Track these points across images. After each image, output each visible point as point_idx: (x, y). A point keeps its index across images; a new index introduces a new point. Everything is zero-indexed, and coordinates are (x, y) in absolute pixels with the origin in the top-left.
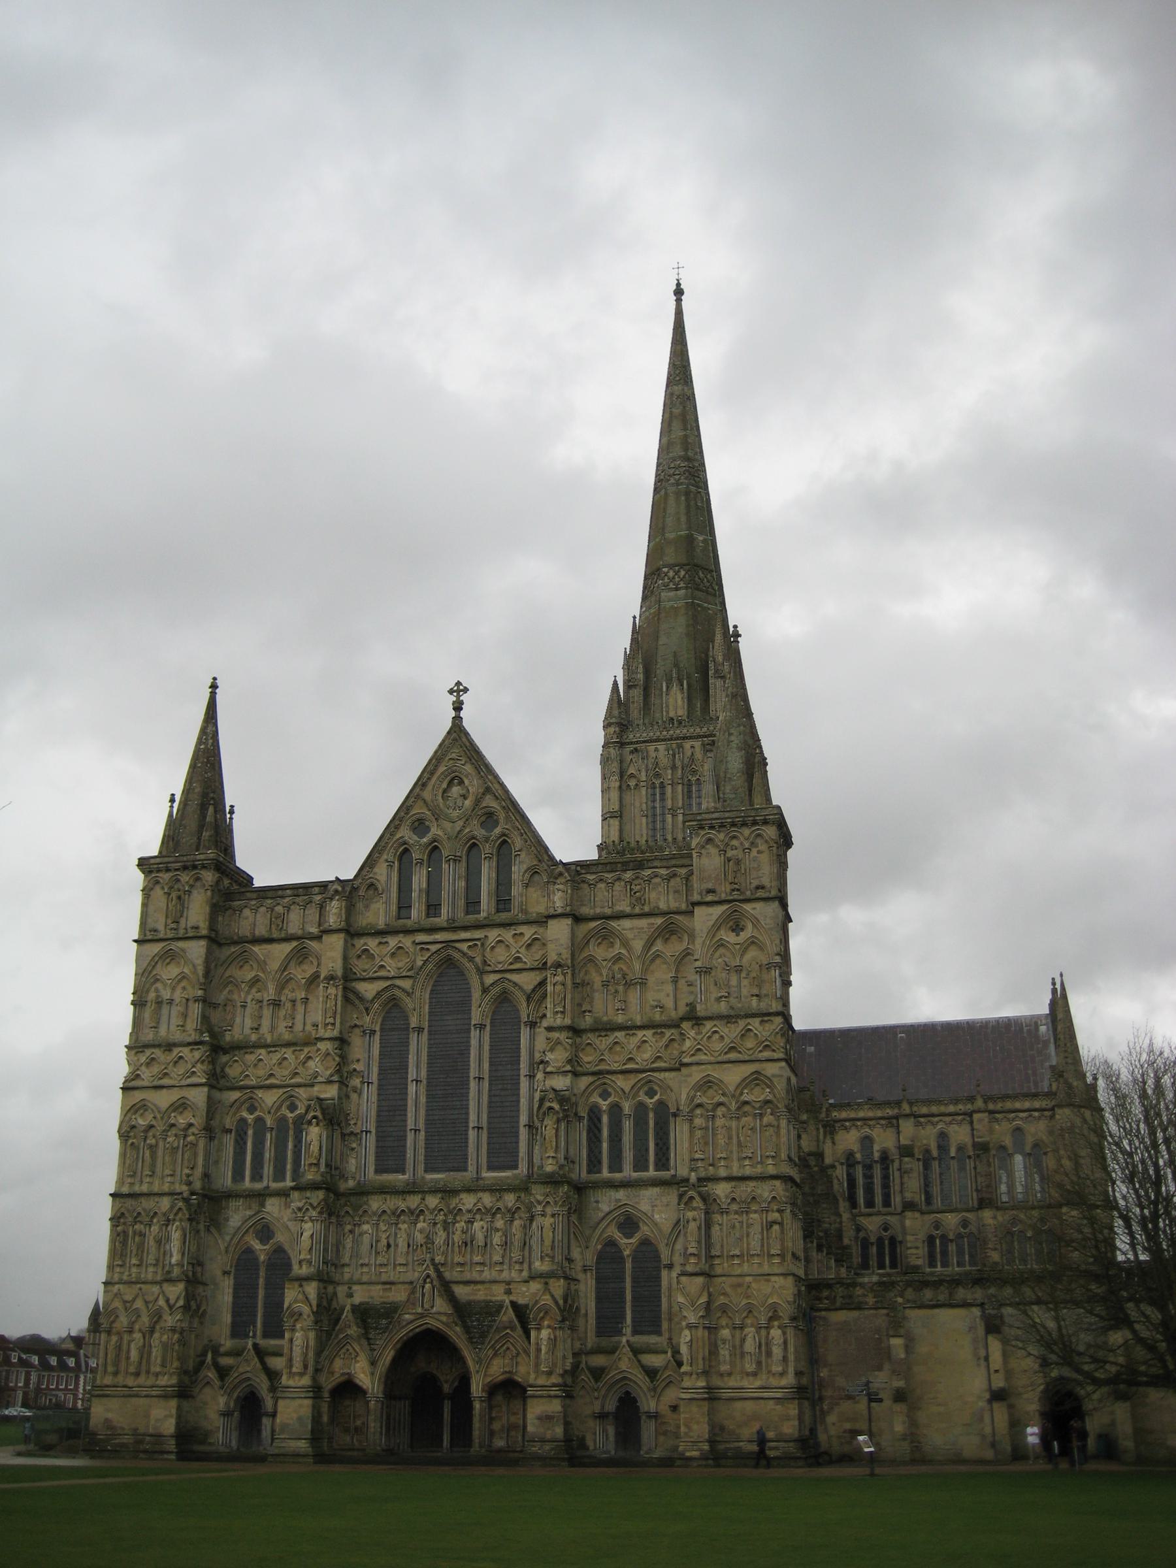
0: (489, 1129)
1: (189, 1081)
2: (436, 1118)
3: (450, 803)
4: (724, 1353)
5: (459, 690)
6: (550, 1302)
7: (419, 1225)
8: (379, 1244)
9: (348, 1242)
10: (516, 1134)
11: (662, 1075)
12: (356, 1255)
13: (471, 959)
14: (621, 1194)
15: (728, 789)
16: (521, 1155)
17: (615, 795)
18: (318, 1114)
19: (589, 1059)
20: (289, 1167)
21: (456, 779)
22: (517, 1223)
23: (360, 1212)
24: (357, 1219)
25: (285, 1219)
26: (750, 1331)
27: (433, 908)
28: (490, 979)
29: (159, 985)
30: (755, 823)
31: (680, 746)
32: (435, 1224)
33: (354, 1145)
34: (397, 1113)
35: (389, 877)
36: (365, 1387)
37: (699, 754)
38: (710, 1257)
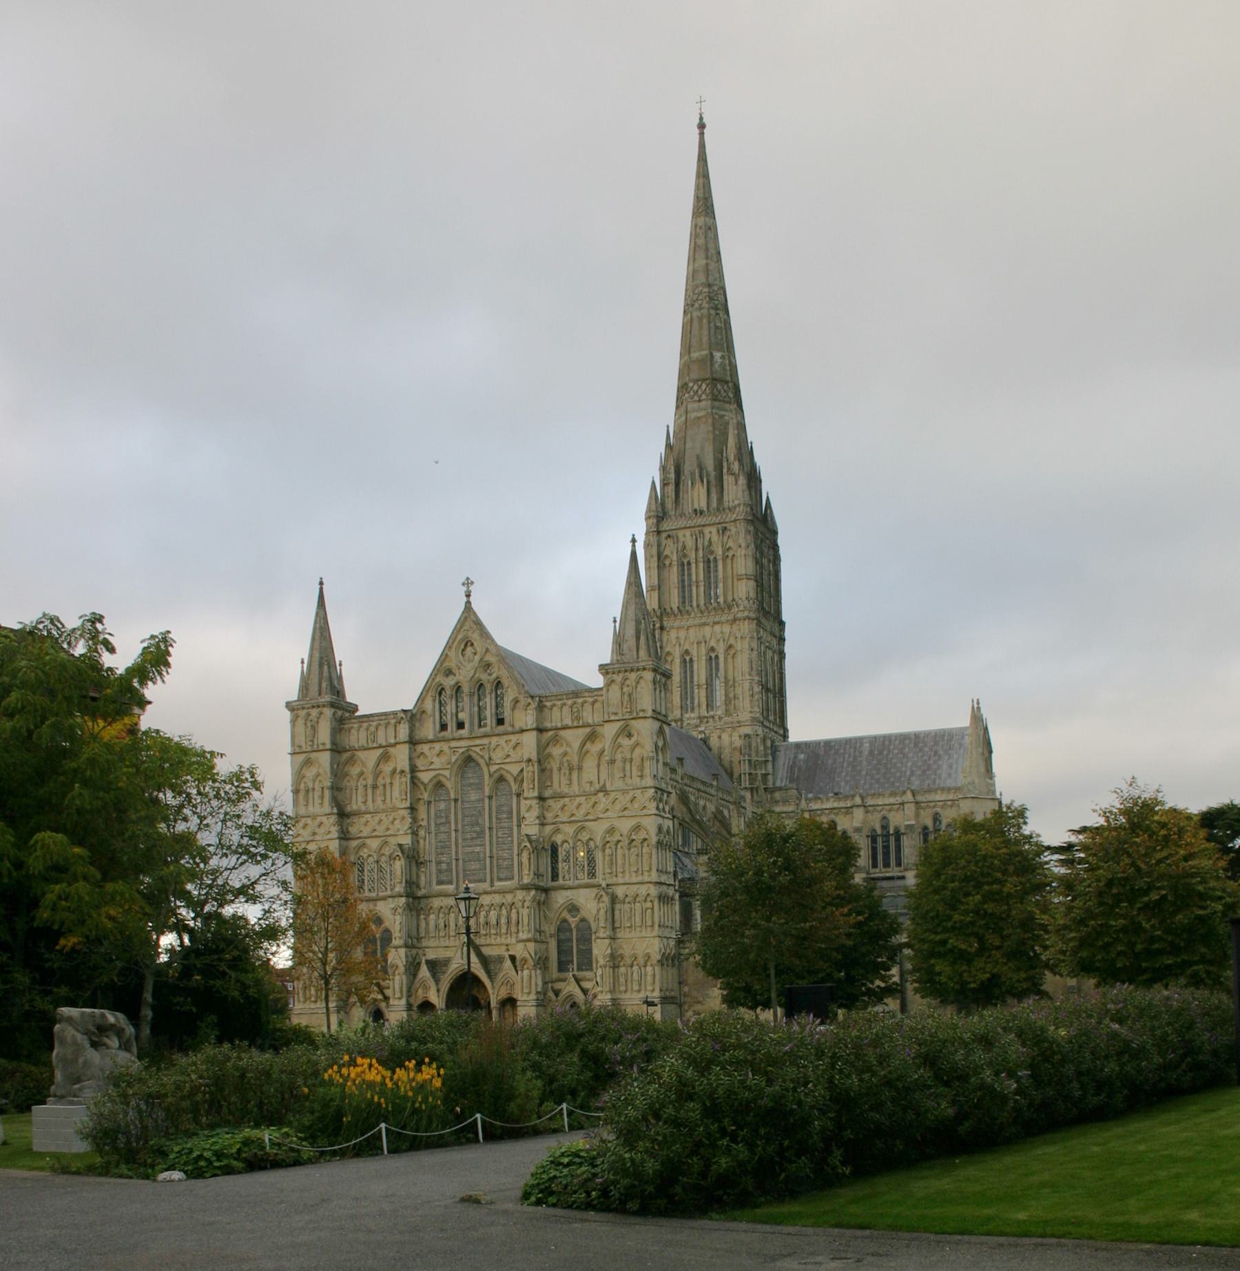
1: (329, 836)
3: (466, 657)
4: (622, 980)
5: (468, 583)
6: (528, 956)
12: (427, 932)
13: (482, 757)
14: (569, 893)
15: (625, 646)
17: (655, 572)
18: (400, 854)
21: (468, 643)
26: (635, 968)
27: (461, 725)
28: (493, 768)
29: (305, 780)
30: (638, 670)
31: (701, 532)
35: (434, 707)
37: (715, 538)
38: (614, 929)
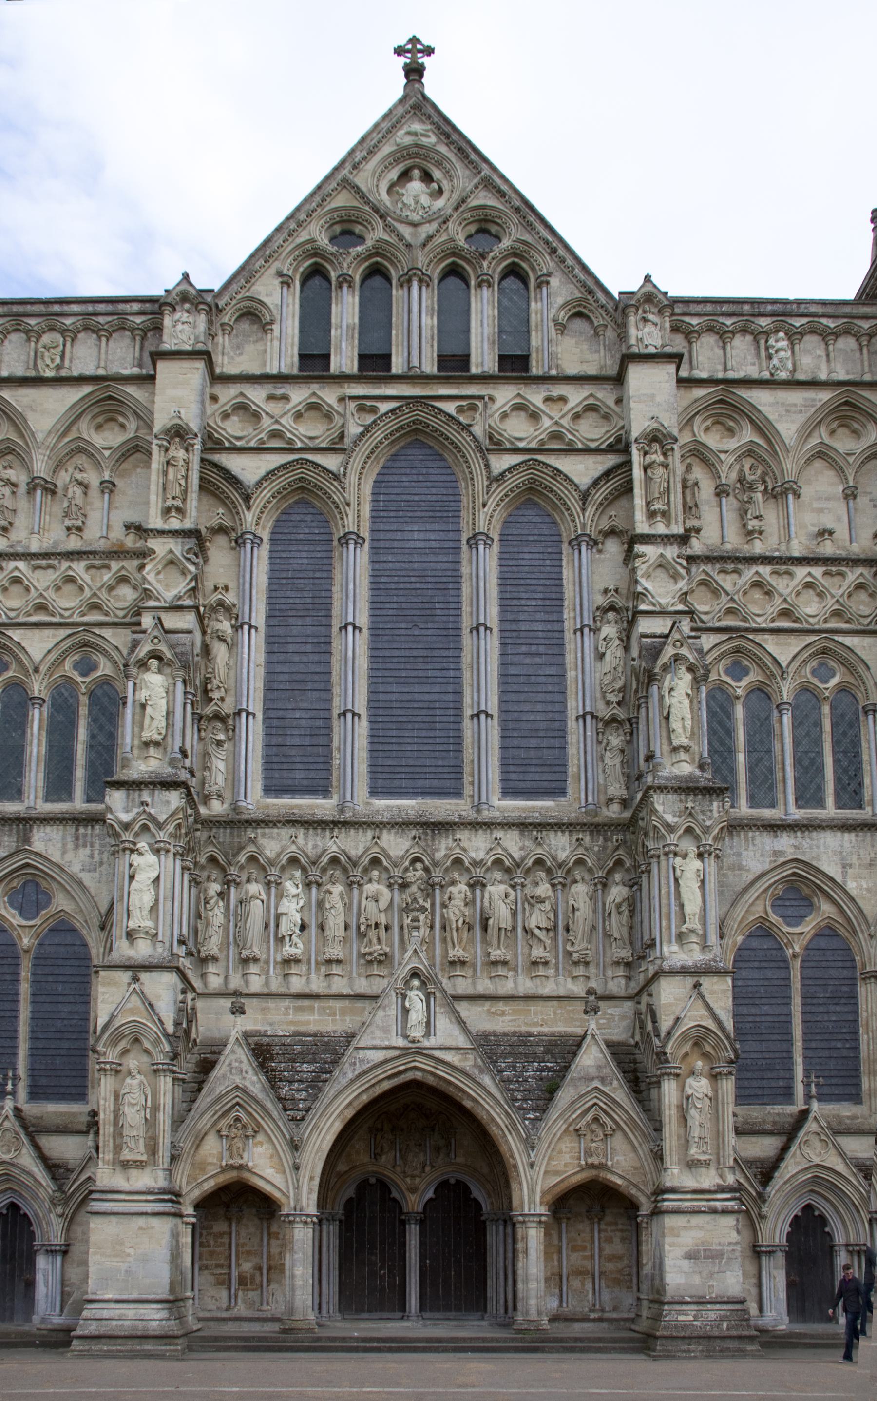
0: (503, 722)
2: (394, 697)
7: (370, 888)
8: (284, 921)
9: (217, 915)
10: (562, 734)
11: (848, 640)
16: (572, 769)
19: (706, 608)
20: (80, 773)
22: (580, 891)
23: (242, 858)
24: (233, 870)
25: (75, 869)
32: (404, 886)
33: (221, 737)
34: (310, 686)
36: (277, 1194)
